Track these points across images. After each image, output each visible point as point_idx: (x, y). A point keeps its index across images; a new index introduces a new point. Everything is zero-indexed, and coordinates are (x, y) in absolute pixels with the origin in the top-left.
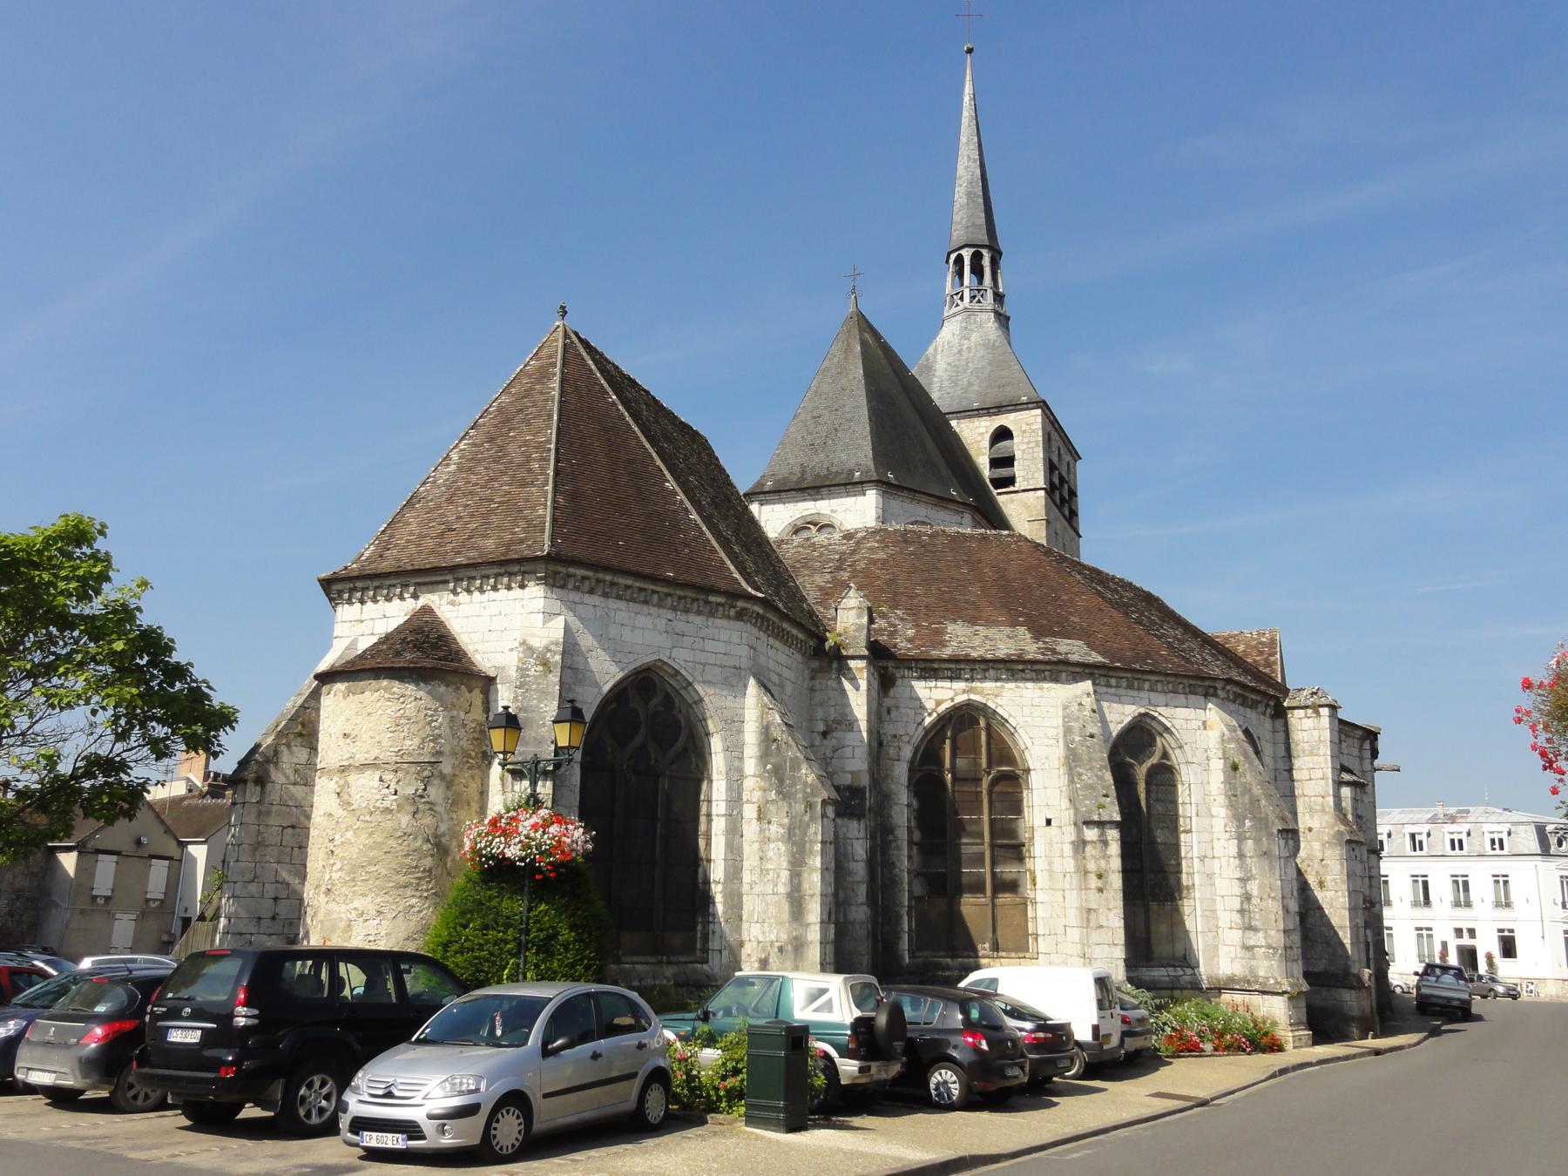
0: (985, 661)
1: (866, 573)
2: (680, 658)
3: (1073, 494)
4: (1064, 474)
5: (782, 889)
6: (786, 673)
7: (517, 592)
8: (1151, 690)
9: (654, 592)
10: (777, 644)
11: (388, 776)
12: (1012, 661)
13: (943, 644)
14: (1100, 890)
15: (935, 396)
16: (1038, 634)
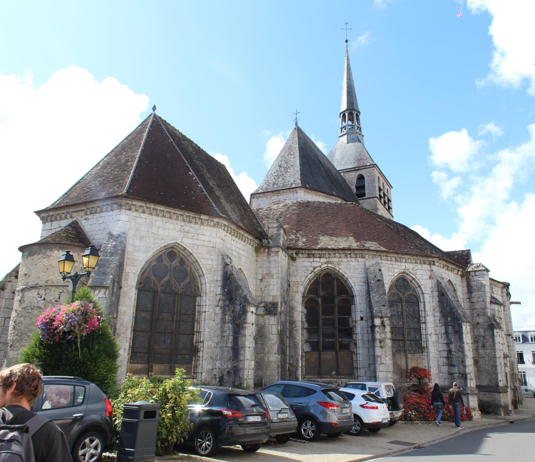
0: (333, 250)
1: (289, 218)
2: (187, 242)
3: (389, 200)
4: (386, 193)
5: (230, 345)
6: (242, 253)
8: (406, 262)
9: (174, 213)
10: (237, 239)
11: (42, 292)
12: (346, 250)
13: (318, 244)
14: (382, 347)
15: (335, 164)
16: (358, 239)
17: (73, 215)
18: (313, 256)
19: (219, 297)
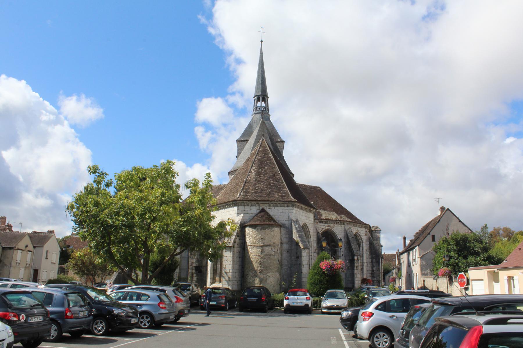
0: (330, 220)
7: (287, 208)
11: (273, 248)
17: (261, 205)
18: (322, 222)
19: (315, 248)
